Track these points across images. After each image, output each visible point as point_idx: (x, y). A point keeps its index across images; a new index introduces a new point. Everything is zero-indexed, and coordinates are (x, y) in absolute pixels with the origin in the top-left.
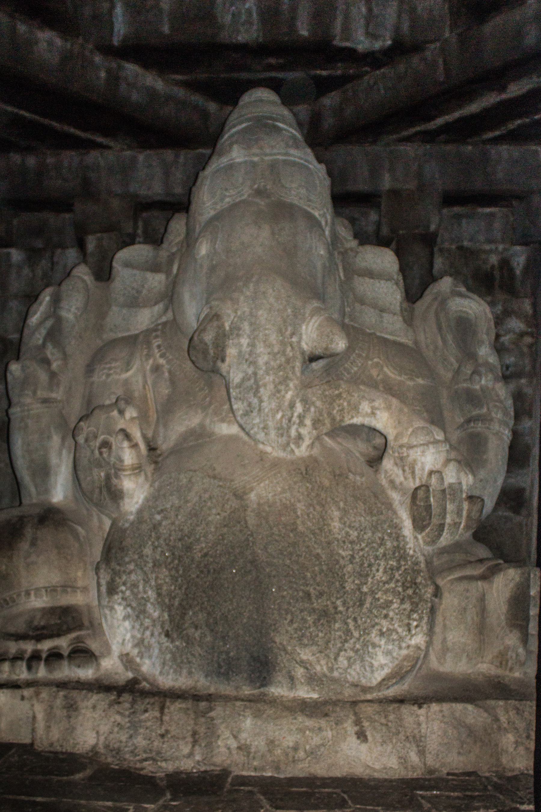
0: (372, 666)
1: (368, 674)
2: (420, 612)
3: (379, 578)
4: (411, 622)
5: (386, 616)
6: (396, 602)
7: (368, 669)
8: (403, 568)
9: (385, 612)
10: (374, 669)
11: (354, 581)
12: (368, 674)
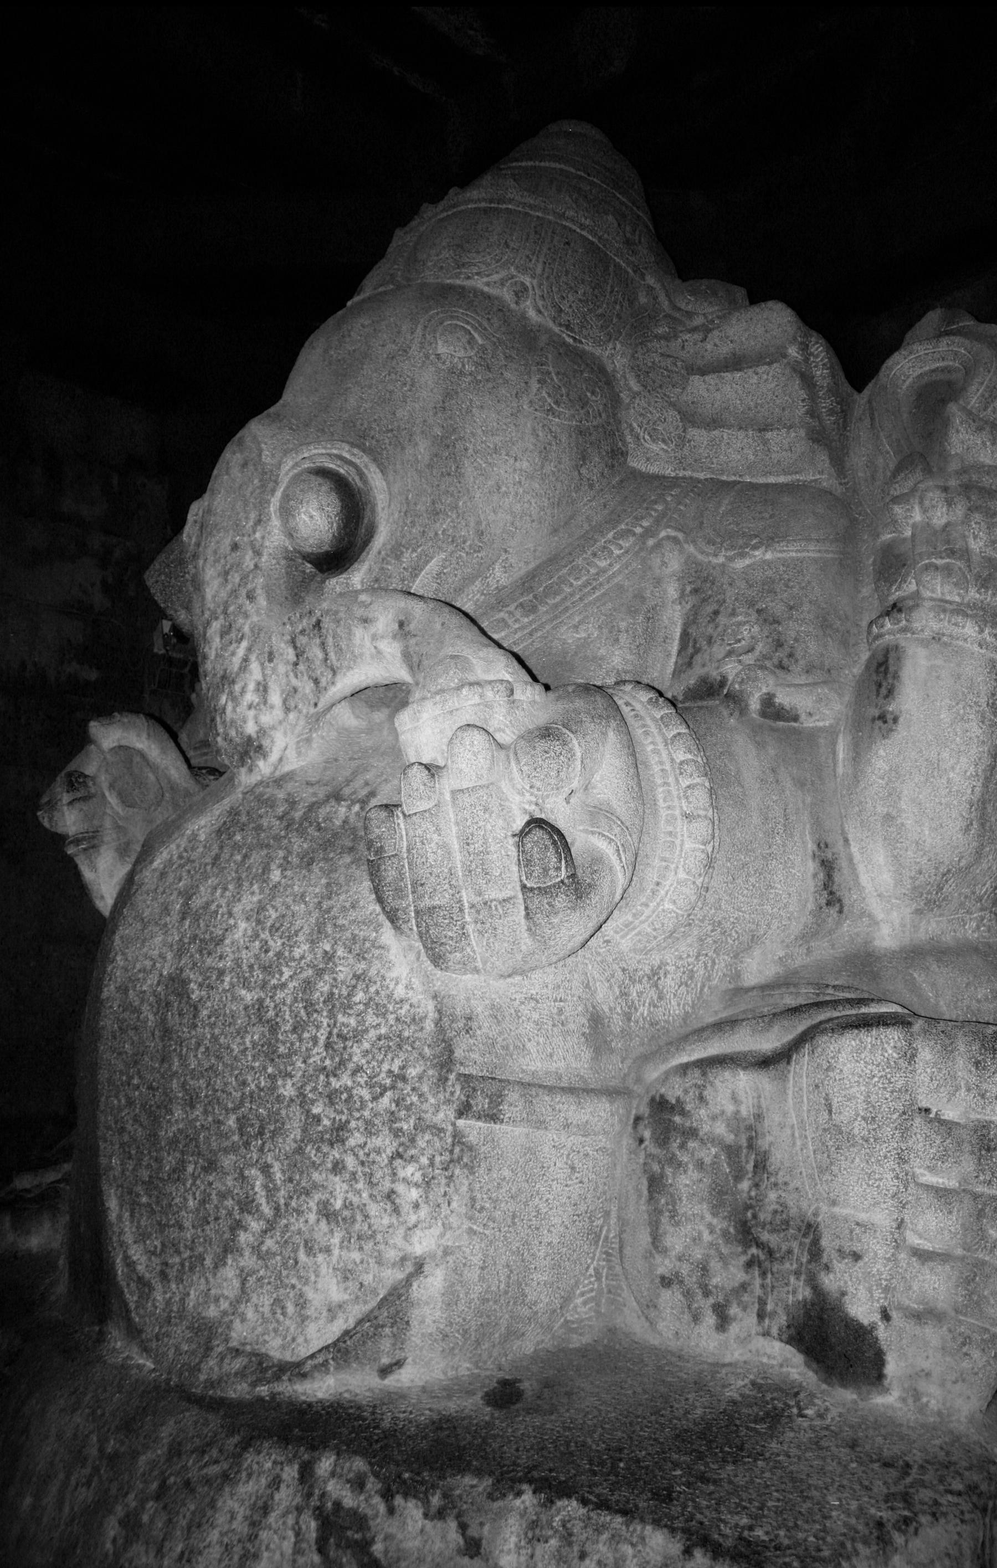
0: (302, 1303)
1: (291, 1325)
2: (424, 1161)
3: (317, 1058)
4: (400, 1188)
5: (338, 1167)
6: (358, 1129)
7: (290, 1309)
8: (372, 1034)
9: (335, 1154)
10: (310, 1312)
11: (265, 1068)
12: (291, 1325)
